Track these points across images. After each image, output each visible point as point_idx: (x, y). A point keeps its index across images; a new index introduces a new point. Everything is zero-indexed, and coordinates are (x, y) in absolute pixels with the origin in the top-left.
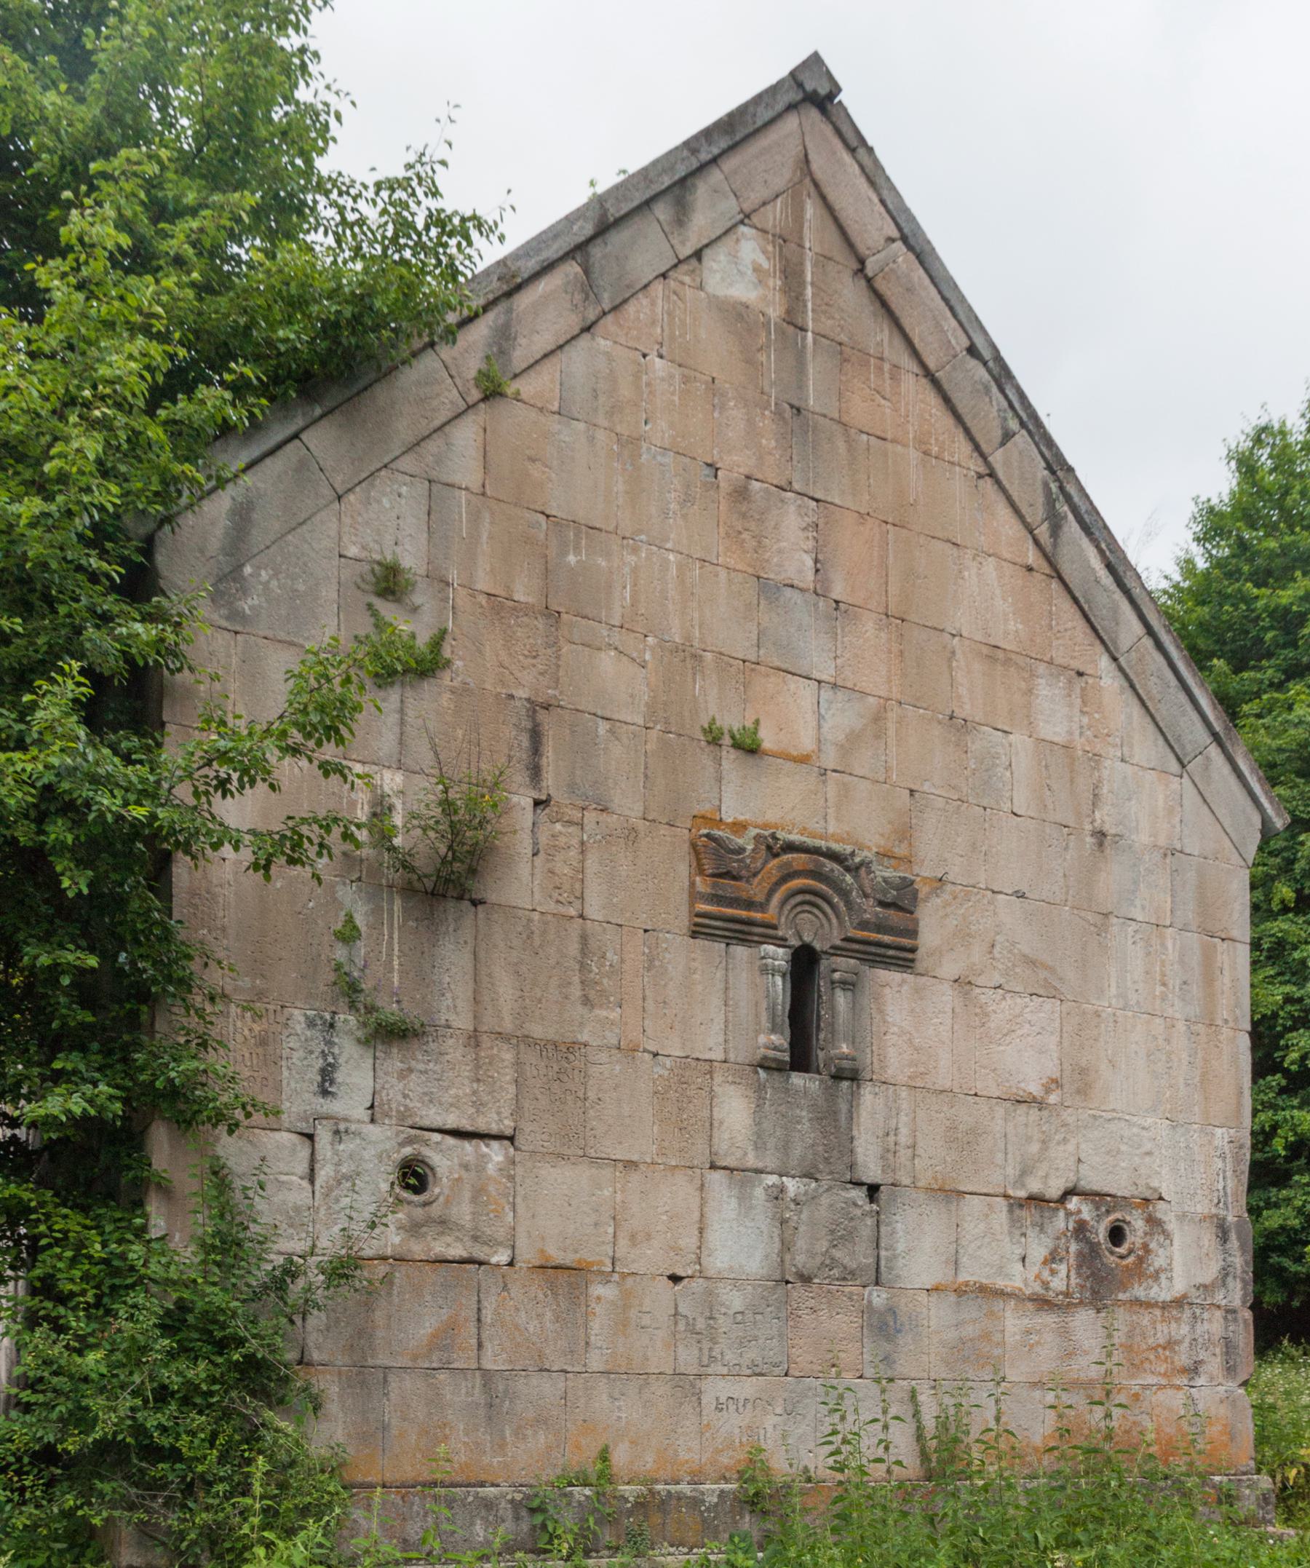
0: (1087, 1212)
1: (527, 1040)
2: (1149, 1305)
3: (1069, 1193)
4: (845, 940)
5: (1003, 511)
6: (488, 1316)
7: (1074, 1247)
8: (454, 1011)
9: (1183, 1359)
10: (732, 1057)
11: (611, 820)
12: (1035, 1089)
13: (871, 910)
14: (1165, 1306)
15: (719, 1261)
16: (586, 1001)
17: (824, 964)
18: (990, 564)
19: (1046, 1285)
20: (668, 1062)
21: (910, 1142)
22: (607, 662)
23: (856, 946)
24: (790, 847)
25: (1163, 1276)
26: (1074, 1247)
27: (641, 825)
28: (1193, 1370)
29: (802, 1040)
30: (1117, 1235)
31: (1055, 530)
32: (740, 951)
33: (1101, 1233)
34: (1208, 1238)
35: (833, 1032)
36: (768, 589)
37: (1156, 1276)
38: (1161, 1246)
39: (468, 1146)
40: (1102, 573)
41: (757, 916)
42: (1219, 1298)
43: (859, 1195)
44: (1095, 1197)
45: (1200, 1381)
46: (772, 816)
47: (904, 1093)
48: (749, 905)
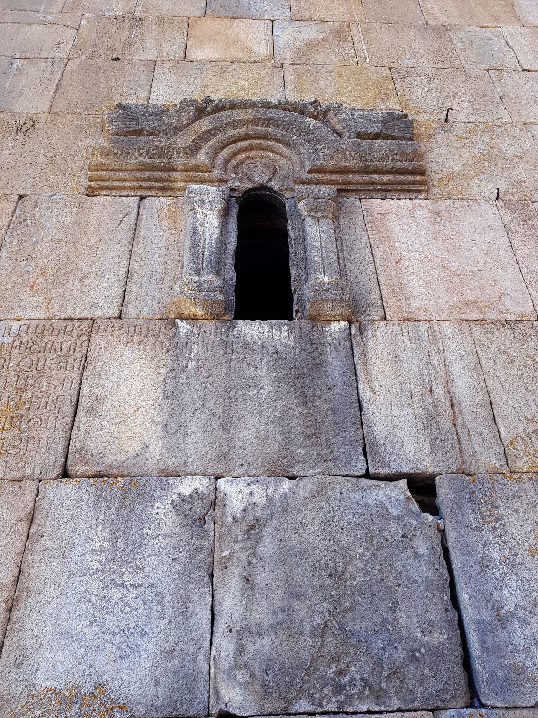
4: (310, 171)
10: (131, 310)
20: (16, 325)
21: (480, 397)
23: (333, 177)
27: (42, 119)
35: (305, 263)
47: (448, 329)
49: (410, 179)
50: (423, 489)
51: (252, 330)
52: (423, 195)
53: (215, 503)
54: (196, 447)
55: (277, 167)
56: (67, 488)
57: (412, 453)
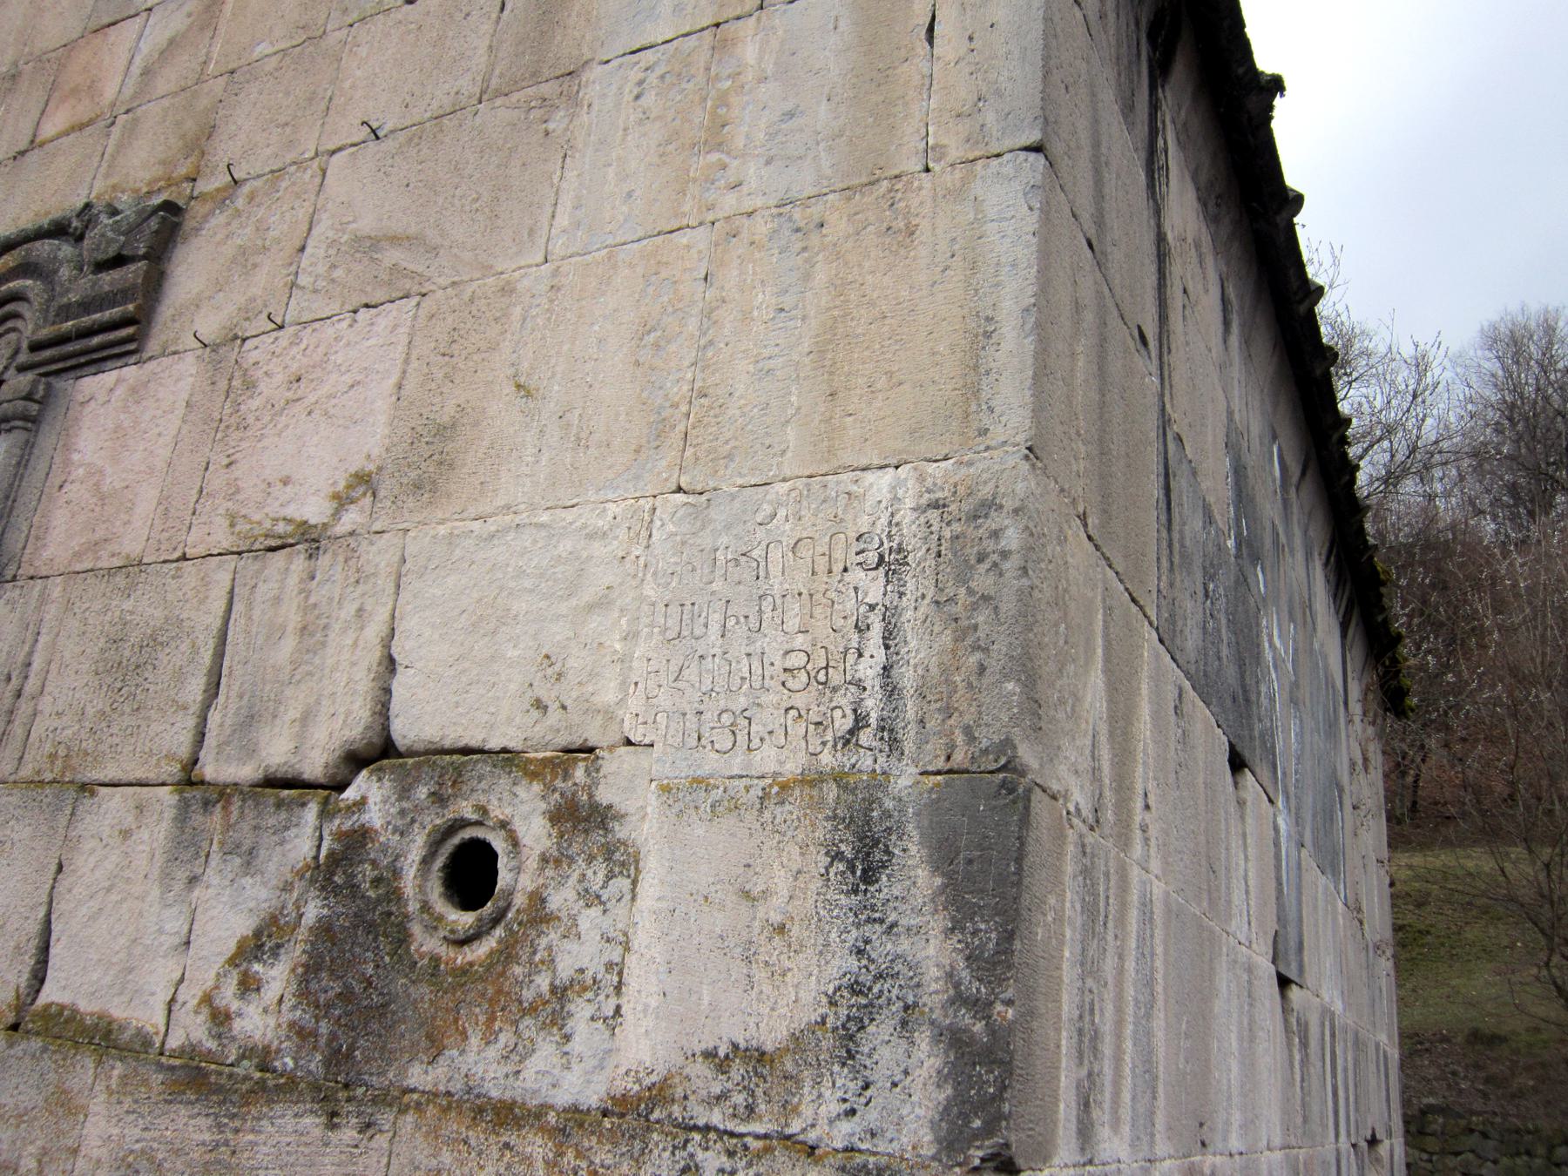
2: (506, 1115)
12: (314, 510)
14: (574, 1123)
19: (221, 1019)
25: (580, 1010)
30: (471, 873)
34: (794, 870)
38: (591, 899)
52: (133, 359)
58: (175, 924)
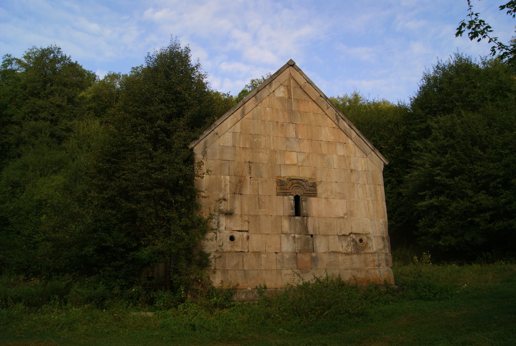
0: (354, 237)
1: (250, 215)
3: (350, 234)
5: (329, 119)
6: (244, 261)
7: (352, 243)
8: (237, 211)
9: (376, 263)
11: (263, 179)
12: (342, 215)
13: (308, 188)
14: (372, 253)
15: (284, 249)
16: (259, 208)
17: (300, 198)
18: (327, 129)
19: (347, 251)
22: (261, 154)
24: (293, 179)
26: (352, 243)
28: (379, 265)
29: (297, 210)
30: (361, 241)
31: (338, 121)
32: (285, 197)
33: (358, 240)
34: (380, 240)
36: (287, 139)
37: (370, 248)
39: (241, 233)
40: (348, 127)
41: (288, 191)
42: (384, 251)
43: (309, 236)
44: (356, 234)
45: (381, 267)
46: (290, 175)
47: (316, 218)
48: (286, 190)
49: (315, 195)
50: (312, 236)
51: (297, 218)
53: (295, 237)
54: (292, 231)
55: (299, 192)
56: (283, 235)
57: (311, 232)
58: (341, 245)
